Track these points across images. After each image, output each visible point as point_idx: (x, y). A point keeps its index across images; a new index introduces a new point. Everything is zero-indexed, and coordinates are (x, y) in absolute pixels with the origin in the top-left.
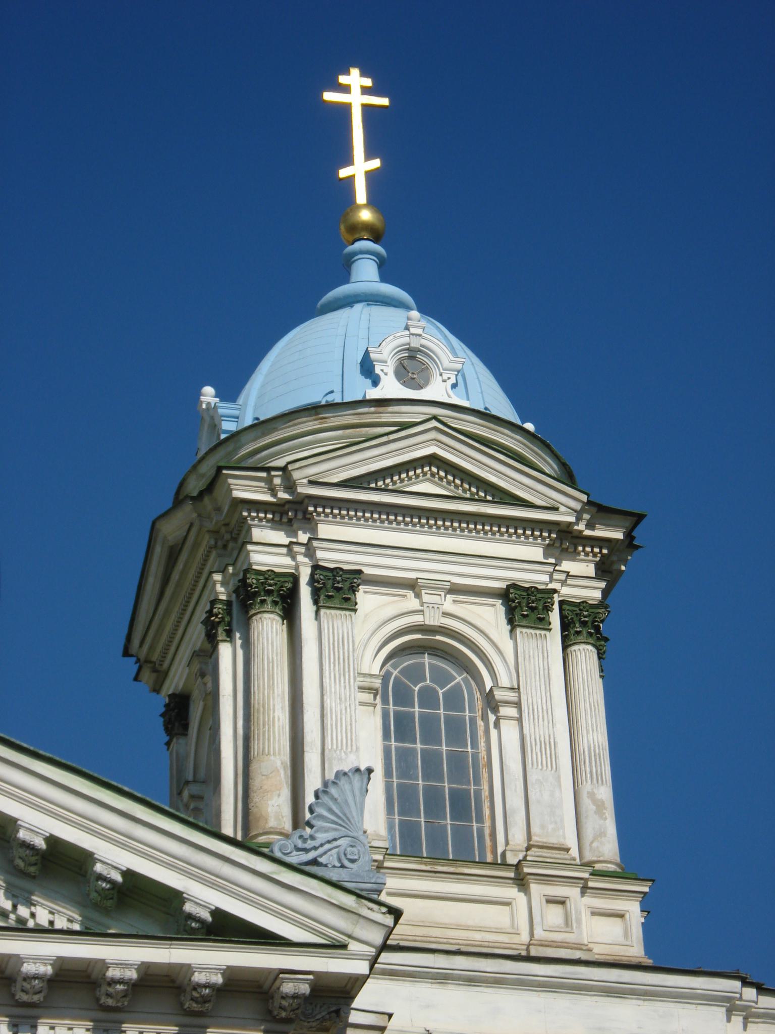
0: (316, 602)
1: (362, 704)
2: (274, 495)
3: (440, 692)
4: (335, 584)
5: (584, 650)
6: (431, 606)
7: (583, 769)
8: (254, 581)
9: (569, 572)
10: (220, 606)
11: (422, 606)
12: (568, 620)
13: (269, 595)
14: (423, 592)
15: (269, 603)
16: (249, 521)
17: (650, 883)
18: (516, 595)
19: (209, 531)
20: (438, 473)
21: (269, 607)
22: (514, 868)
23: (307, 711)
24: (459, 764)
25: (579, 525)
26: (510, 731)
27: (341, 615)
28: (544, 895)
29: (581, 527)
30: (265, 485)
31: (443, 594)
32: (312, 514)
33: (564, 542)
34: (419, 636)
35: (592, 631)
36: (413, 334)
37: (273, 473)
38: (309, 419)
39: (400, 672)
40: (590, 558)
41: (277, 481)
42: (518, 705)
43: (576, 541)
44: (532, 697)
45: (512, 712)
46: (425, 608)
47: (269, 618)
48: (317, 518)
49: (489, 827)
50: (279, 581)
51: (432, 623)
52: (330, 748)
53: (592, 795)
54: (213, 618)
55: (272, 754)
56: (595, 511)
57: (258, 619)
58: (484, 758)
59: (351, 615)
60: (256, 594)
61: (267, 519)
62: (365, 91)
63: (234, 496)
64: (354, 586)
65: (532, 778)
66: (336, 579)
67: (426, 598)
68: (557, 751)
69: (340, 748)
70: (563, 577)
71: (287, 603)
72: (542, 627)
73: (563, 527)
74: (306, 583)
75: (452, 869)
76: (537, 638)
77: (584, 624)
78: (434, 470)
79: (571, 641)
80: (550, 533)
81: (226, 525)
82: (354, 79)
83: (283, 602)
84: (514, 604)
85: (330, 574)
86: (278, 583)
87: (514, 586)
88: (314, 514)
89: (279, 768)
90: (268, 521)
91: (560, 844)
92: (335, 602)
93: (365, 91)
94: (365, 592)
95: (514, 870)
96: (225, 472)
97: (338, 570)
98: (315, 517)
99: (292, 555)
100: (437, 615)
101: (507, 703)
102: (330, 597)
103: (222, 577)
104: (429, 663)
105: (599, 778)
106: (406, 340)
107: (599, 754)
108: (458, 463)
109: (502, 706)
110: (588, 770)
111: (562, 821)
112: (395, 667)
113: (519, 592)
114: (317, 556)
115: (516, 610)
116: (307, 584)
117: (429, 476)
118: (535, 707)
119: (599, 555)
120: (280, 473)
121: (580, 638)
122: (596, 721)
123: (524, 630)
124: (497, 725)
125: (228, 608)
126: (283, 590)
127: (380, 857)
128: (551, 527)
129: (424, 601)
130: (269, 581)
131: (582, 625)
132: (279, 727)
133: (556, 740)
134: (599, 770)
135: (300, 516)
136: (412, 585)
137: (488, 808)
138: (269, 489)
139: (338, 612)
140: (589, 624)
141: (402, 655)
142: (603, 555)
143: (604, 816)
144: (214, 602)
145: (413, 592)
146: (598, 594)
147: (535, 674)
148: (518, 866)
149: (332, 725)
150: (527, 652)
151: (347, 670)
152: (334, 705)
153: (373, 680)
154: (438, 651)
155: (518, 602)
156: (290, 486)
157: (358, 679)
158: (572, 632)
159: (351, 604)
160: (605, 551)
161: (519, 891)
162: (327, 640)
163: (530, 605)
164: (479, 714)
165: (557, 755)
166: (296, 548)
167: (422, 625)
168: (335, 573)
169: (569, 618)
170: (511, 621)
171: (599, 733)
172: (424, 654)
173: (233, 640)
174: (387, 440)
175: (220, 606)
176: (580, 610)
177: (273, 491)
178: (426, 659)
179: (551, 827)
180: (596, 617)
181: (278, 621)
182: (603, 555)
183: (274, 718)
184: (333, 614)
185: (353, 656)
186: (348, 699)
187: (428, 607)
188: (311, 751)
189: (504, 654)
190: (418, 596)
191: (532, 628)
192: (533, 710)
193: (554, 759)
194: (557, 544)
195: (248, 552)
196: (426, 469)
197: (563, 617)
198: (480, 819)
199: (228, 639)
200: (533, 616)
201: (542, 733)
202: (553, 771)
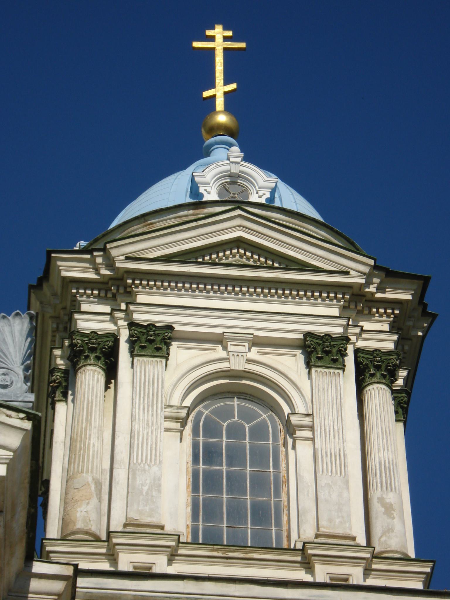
0: (132, 355)
1: (167, 430)
2: (98, 273)
3: (247, 426)
4: (148, 337)
5: (377, 388)
6: (236, 354)
7: (375, 480)
8: (79, 341)
10: (59, 374)
11: (228, 355)
12: (363, 366)
13: (92, 353)
14: (229, 343)
15: (92, 358)
16: (78, 298)
17: (431, 564)
18: (312, 342)
19: (51, 317)
20: (245, 254)
21: (92, 361)
22: (301, 552)
23: (119, 437)
25: (370, 288)
27: (153, 361)
28: (327, 573)
29: (372, 289)
30: (90, 265)
31: (247, 345)
32: (131, 287)
33: (358, 304)
35: (385, 373)
37: (95, 254)
38: (139, 226)
39: (212, 412)
40: (384, 319)
41: (99, 260)
42: (312, 428)
43: (370, 304)
44: (324, 420)
45: (308, 434)
46: (230, 356)
47: (91, 370)
49: (287, 530)
50: (102, 341)
51: (237, 368)
52: (135, 462)
53: (381, 500)
55: (85, 472)
56: (384, 276)
57: (81, 371)
58: (284, 476)
59: (161, 361)
60: (81, 352)
61: (94, 295)
63: (62, 275)
64: (165, 339)
65: (322, 482)
66: (149, 333)
67: (231, 348)
68: (346, 461)
69: (144, 462)
70: (357, 330)
71: (111, 361)
72: (335, 366)
73: (356, 291)
74: (125, 341)
75: (242, 555)
76: (331, 375)
77: (378, 368)
78: (242, 251)
79: (366, 383)
80: (344, 294)
83: (106, 359)
84: (309, 349)
85: (145, 331)
86: (101, 343)
87: (308, 335)
88: (133, 286)
89: (90, 483)
90: (95, 297)
91: (346, 534)
92: (148, 351)
94: (179, 348)
95: (301, 554)
96: (53, 255)
97: (151, 326)
98: (134, 288)
99: (114, 320)
100: (242, 361)
101: (303, 427)
102: (143, 348)
103: (61, 352)
104: (238, 405)
105: (389, 486)
107: (389, 468)
108: (261, 243)
109: (298, 430)
110: (379, 480)
111: (349, 516)
112: (205, 408)
113: (315, 341)
114: (134, 317)
115: (312, 355)
116: (126, 341)
117: (237, 257)
118: (327, 428)
119: (392, 316)
120: (101, 253)
121: (374, 380)
122: (387, 442)
123: (319, 370)
124: (294, 447)
125: (66, 376)
126: (105, 348)
127: (173, 543)
128: (345, 290)
129: (229, 351)
130: (92, 341)
131: (376, 370)
132: (94, 451)
133: (345, 453)
134: (388, 480)
135: (121, 290)
137: (286, 515)
138: (93, 269)
139: (150, 359)
140: (383, 368)
141: (213, 399)
142: (396, 316)
143: (393, 516)
144: (52, 372)
145: (221, 346)
146: (391, 346)
147: (328, 402)
148: (303, 550)
149: (138, 444)
150: (321, 386)
151: (155, 402)
152: (141, 429)
153: (179, 411)
154: (247, 396)
155: (313, 348)
156: (110, 263)
157: (166, 410)
158: (368, 375)
159: (162, 352)
160: (397, 312)
161: (306, 573)
162: (138, 380)
163: (325, 349)
164: (281, 442)
165: (346, 464)
166: (117, 314)
168: (149, 329)
169: (364, 364)
170: (309, 365)
171: (390, 452)
172: (234, 398)
174: (196, 225)
175: (59, 374)
177: (96, 270)
179: (337, 521)
180: (389, 363)
181: (100, 372)
182: (396, 316)
183: (89, 444)
184: (145, 361)
185: (162, 392)
186: (155, 424)
187: (233, 355)
188: (119, 468)
189: (301, 390)
190: (225, 348)
191: (326, 367)
192: (325, 430)
193: (343, 468)
194: (352, 306)
195: (76, 320)
197: (357, 364)
198: (278, 524)
199: (64, 399)
200: (328, 358)
201: (333, 448)
202: (341, 477)
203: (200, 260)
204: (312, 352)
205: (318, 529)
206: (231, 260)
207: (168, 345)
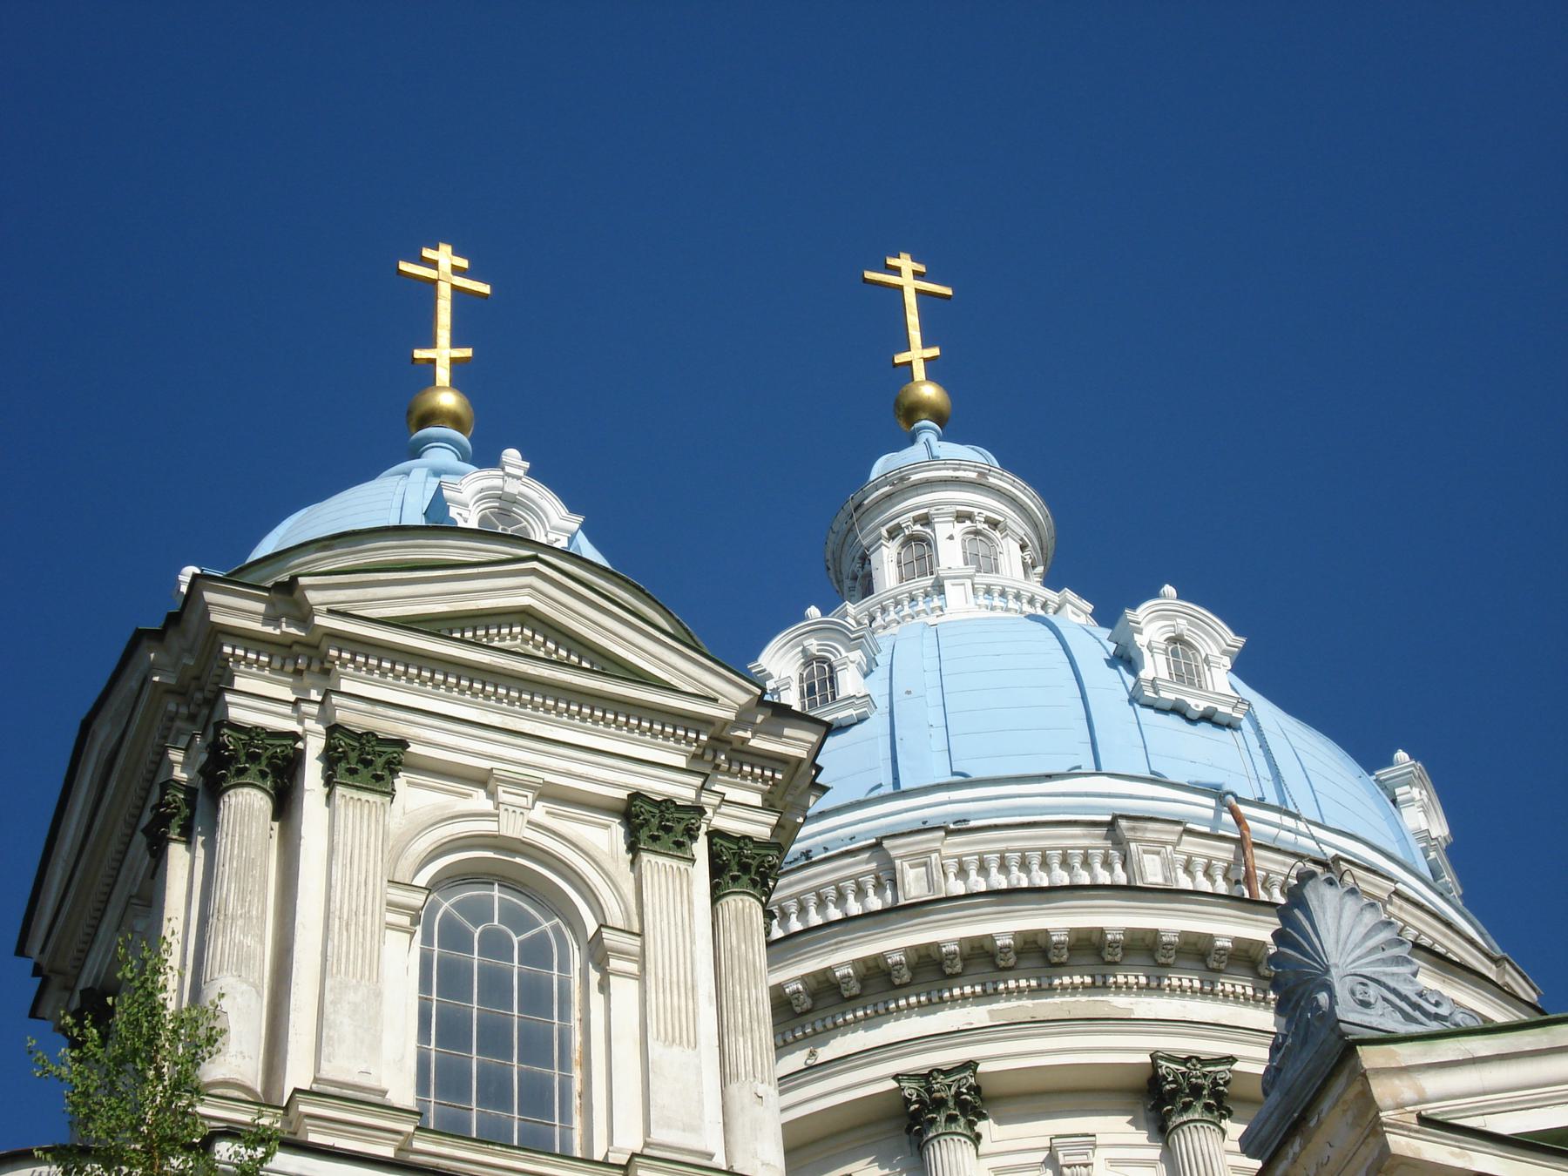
0: (329, 781)
3: (516, 940)
6: (511, 809)
9: (724, 794)
11: (497, 808)
14: (500, 789)
20: (533, 638)
24: (538, 1047)
26: (624, 991)
31: (530, 795)
34: (490, 854)
36: (509, 475)
39: (455, 906)
48: (342, 670)
51: (510, 834)
54: (162, 810)
56: (770, 713)
62: (456, 271)
67: (503, 797)
70: (716, 800)
78: (528, 633)
81: (197, 678)
82: (444, 256)
88: (337, 662)
93: (456, 271)
94: (410, 784)
101: (623, 954)
104: (499, 898)
106: (499, 482)
109: (614, 956)
124: (604, 987)
129: (500, 801)
135: (315, 667)
136: (483, 780)
155: (644, 819)
156: (303, 616)
160: (779, 776)
166: (305, 707)
167: (495, 837)
170: (633, 848)
172: (493, 884)
173: (193, 845)
176: (741, 848)
178: (496, 892)
182: (776, 783)
190: (492, 795)
195: (226, 705)
196: (516, 630)
197: (713, 856)
203: (458, 635)
204: (642, 826)
205: (647, 1131)
206: (507, 644)
207: (394, 773)
